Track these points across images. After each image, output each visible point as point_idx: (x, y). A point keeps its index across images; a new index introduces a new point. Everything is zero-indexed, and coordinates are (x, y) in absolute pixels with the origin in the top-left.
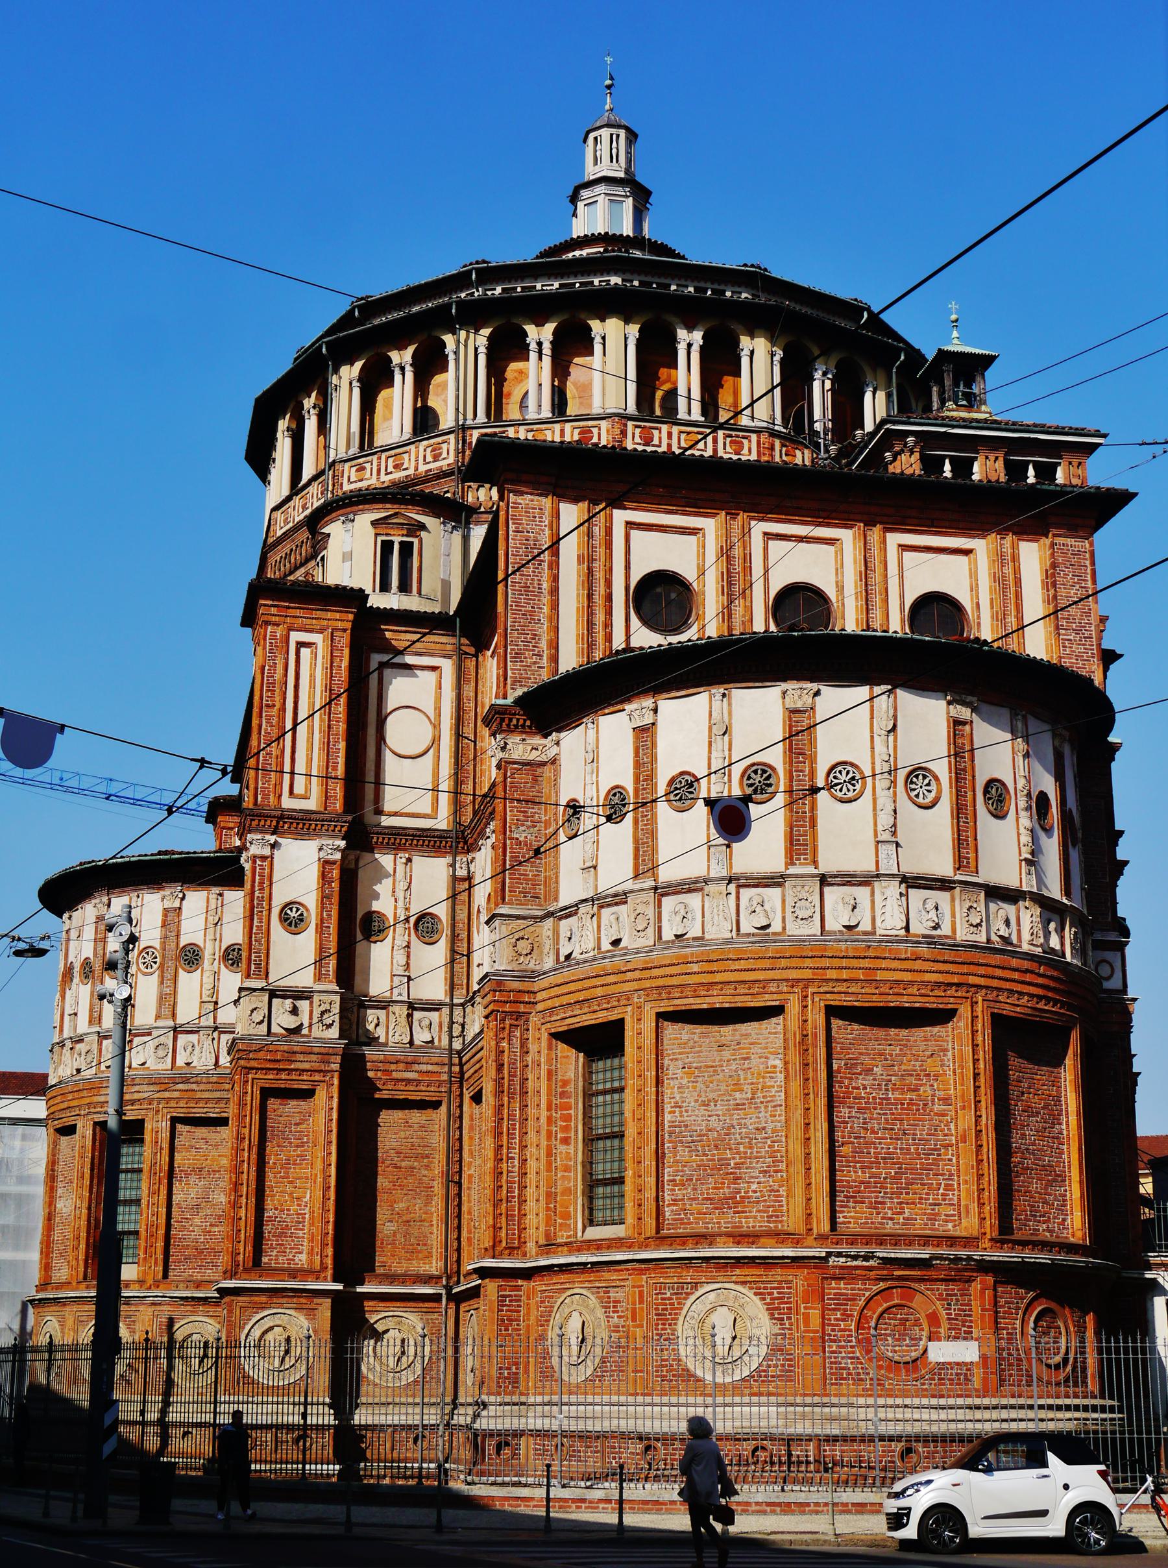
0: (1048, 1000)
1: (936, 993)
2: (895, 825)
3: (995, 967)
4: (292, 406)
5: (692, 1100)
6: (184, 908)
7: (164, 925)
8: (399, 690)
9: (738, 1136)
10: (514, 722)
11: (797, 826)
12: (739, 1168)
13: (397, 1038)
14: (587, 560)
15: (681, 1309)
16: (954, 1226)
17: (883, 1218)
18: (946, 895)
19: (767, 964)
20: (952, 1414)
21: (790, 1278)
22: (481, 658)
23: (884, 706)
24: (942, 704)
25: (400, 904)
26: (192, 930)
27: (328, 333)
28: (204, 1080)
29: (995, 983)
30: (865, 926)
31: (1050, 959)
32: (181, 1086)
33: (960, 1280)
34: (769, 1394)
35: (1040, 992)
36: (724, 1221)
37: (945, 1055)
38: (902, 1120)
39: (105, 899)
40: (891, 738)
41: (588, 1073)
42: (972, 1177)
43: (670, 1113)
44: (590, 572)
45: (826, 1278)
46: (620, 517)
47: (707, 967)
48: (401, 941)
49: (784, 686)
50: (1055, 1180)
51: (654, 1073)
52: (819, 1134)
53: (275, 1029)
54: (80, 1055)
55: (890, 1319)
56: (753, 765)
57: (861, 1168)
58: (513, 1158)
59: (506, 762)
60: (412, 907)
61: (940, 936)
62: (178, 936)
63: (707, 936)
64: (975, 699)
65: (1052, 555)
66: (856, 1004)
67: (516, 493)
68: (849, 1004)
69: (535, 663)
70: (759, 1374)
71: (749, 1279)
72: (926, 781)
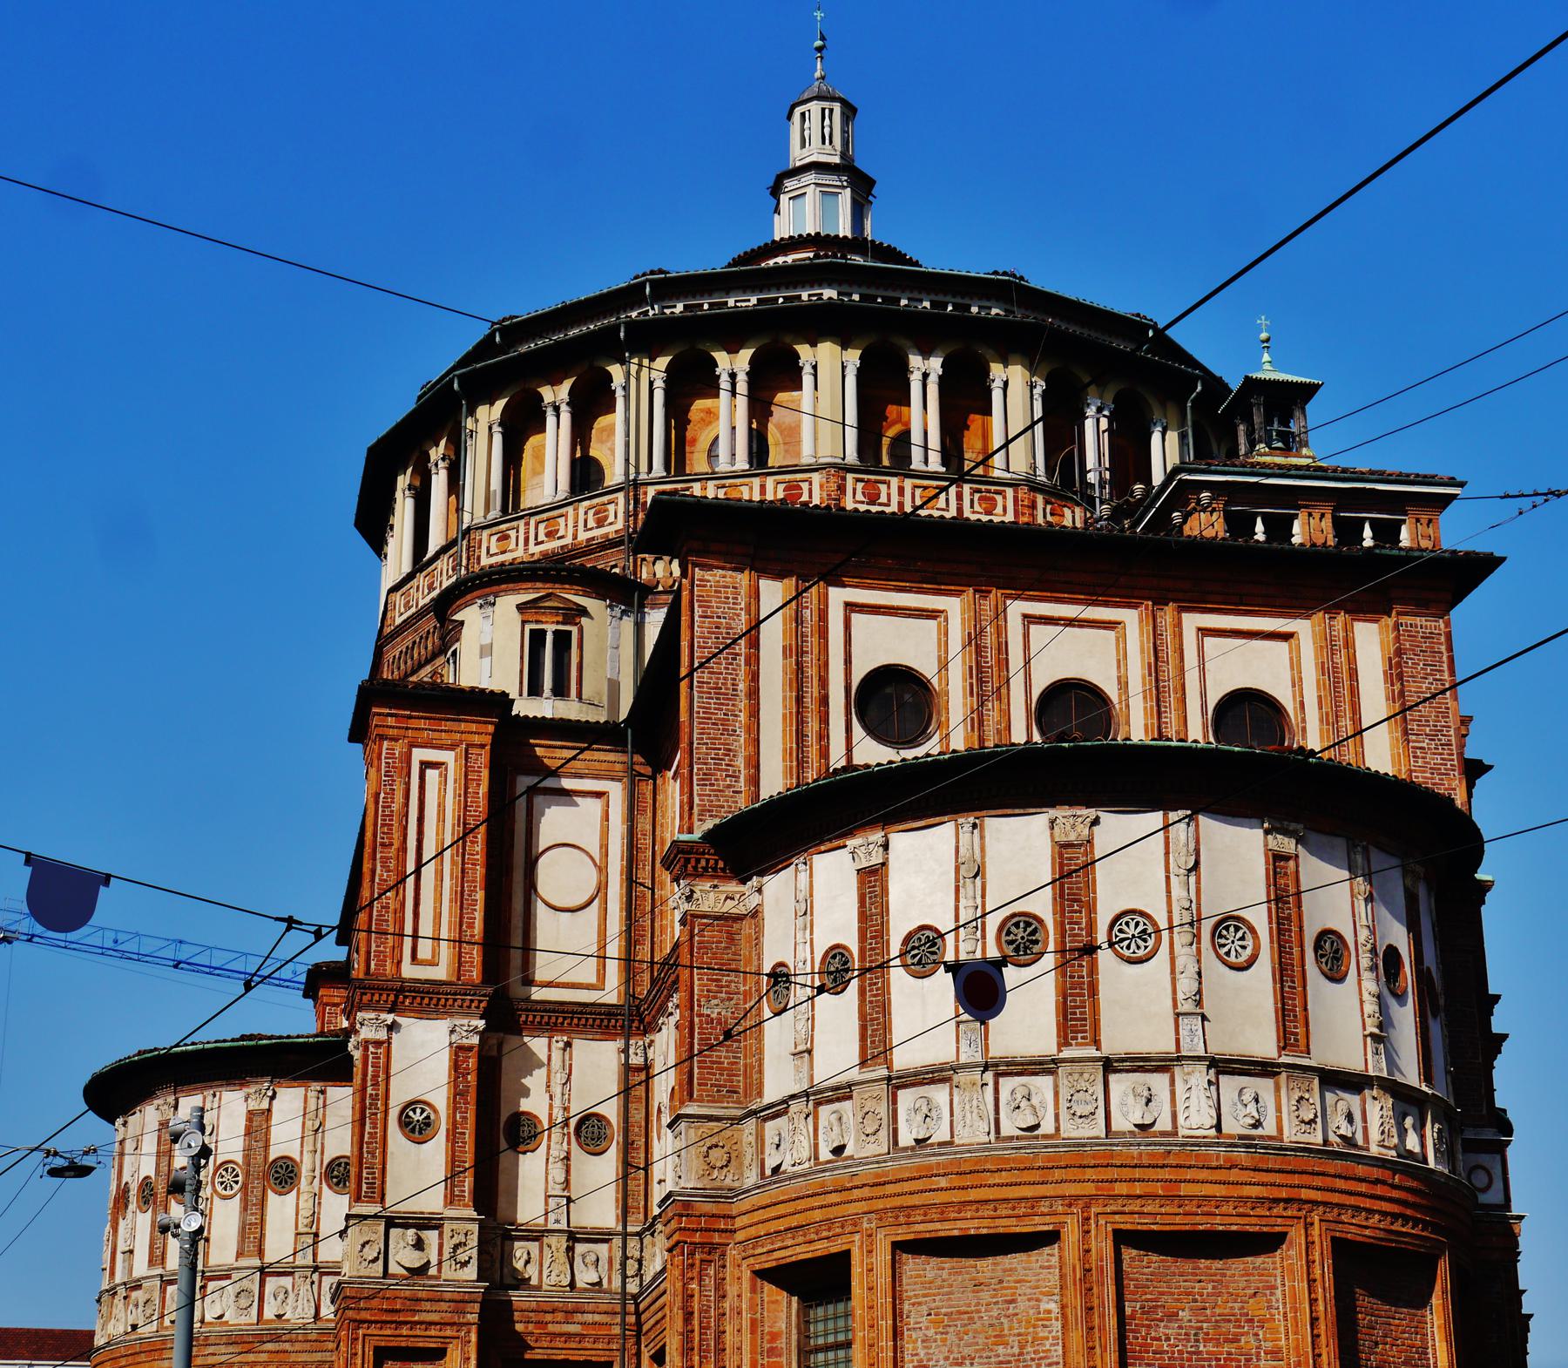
1: (1259, 1211)
2: (1199, 992)
3: (1334, 1176)
4: (414, 458)
5: (941, 1357)
6: (274, 1110)
7: (248, 1133)
8: (554, 823)
10: (703, 863)
11: (1071, 995)
13: (554, 1279)
14: (795, 652)
18: (1268, 1083)
19: (1035, 1176)
22: (659, 781)
23: (1183, 837)
24: (1258, 833)
25: (557, 1102)
26: (285, 1138)
27: (462, 363)
28: (300, 1338)
29: (1336, 1198)
30: (1164, 1124)
31: (1407, 1165)
32: (269, 1346)
35: (1396, 1209)
37: (1272, 1294)
39: (171, 1099)
40: (1192, 879)
41: (804, 1323)
44: (800, 667)
46: (838, 596)
48: (558, 1151)
49: (1053, 813)
51: (890, 1322)
53: (394, 1269)
54: (137, 1306)
56: (1014, 915)
59: (692, 915)
60: (572, 1105)
61: (1261, 1137)
62: (267, 1147)
63: (957, 1141)
64: (1300, 827)
65: (1397, 639)
66: (1154, 1227)
67: (704, 567)
68: (1145, 1228)
69: (729, 786)
72: (1240, 934)
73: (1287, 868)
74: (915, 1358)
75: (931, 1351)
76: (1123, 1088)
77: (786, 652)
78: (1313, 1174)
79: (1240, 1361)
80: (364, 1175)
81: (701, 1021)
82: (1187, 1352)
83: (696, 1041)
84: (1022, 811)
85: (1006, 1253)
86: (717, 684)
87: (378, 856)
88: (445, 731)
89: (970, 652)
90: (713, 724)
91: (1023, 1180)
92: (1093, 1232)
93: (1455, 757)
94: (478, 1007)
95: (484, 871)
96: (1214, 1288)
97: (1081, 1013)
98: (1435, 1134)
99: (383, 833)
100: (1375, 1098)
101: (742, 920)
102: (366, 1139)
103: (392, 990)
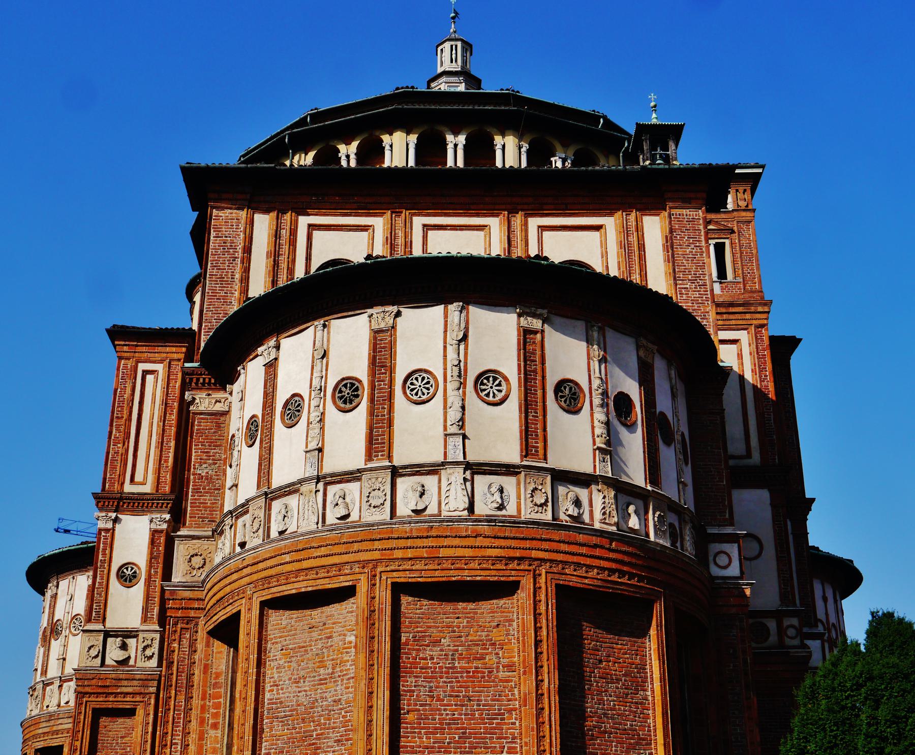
0: (622, 574)
1: (498, 566)
2: (462, 420)
3: (559, 542)
5: (287, 678)
9: (320, 709)
10: (201, 380)
11: (377, 428)
12: (319, 739)
18: (512, 480)
19: (341, 548)
23: (456, 320)
29: (560, 557)
30: (432, 510)
31: (624, 537)
35: (613, 566)
37: (510, 625)
38: (467, 687)
39: (55, 583)
40: (462, 347)
43: (269, 691)
46: (304, 221)
47: (295, 556)
49: (370, 311)
50: (637, 743)
52: (380, 702)
53: (108, 661)
57: (426, 733)
58: (176, 744)
61: (504, 516)
64: (545, 311)
66: (419, 579)
67: (218, 208)
68: (413, 580)
72: (497, 382)
73: (535, 339)
74: (272, 680)
75: (281, 675)
76: (405, 486)
77: (268, 255)
78: (541, 540)
79: (484, 673)
80: (94, 607)
81: (195, 478)
82: (446, 668)
83: (190, 490)
84: (352, 313)
85: (328, 605)
86: (222, 275)
87: (114, 424)
88: (157, 353)
89: (387, 248)
90: (218, 299)
92: (378, 585)
93: (709, 293)
94: (166, 507)
95: (175, 429)
96: (468, 622)
97: (382, 439)
98: (656, 519)
99: (118, 411)
100: (599, 491)
101: (226, 414)
102: (97, 586)
103: (115, 499)
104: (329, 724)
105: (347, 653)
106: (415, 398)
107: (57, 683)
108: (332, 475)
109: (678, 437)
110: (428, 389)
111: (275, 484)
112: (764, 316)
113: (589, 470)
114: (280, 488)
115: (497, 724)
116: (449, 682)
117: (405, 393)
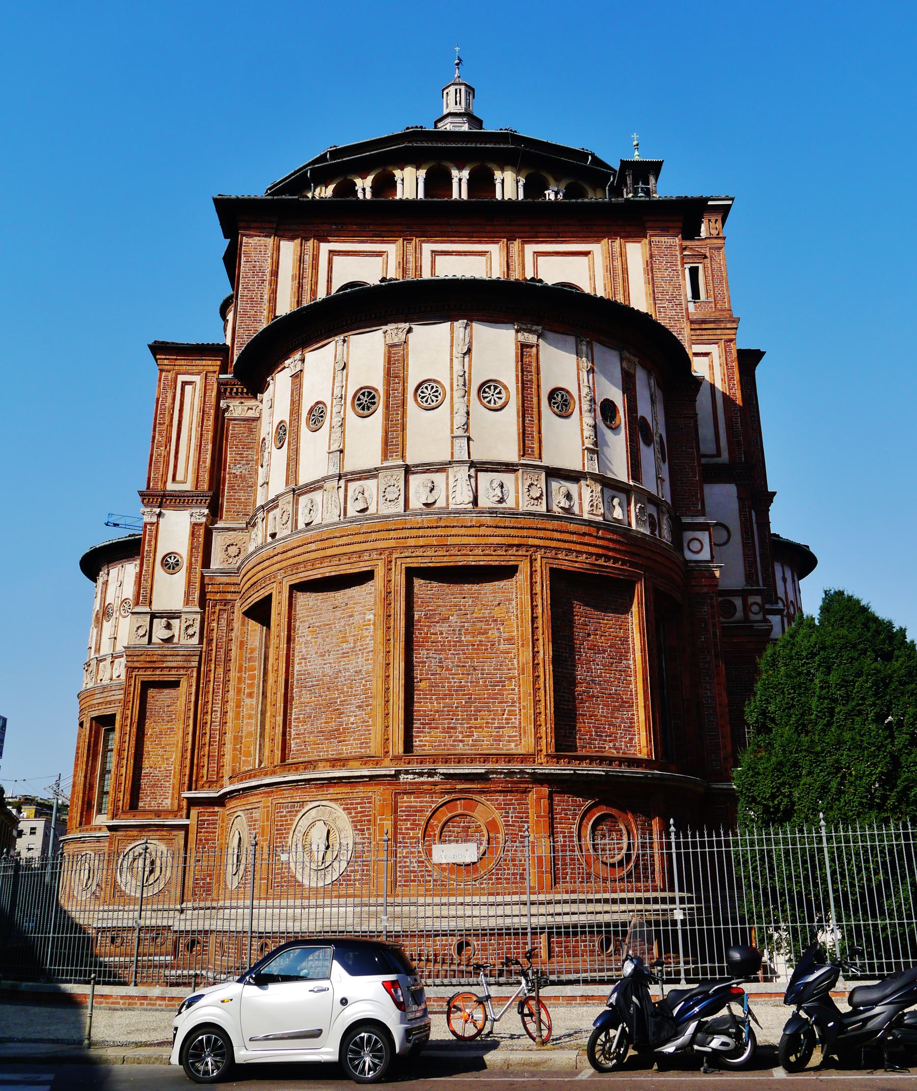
0: (608, 558)
2: (467, 424)
3: (553, 530)
5: (313, 652)
12: (343, 705)
15: (292, 824)
16: (516, 746)
17: (454, 741)
18: (511, 476)
20: (508, 910)
21: (370, 794)
29: (554, 544)
31: (609, 526)
33: (517, 791)
34: (347, 896)
35: (600, 551)
36: (331, 750)
40: (467, 359)
42: (528, 702)
43: (298, 664)
45: (400, 793)
50: (621, 706)
52: (396, 672)
53: (154, 640)
55: (454, 827)
58: (216, 711)
61: (505, 508)
70: (344, 878)
71: (339, 796)
72: (497, 391)
78: (537, 529)
80: (142, 592)
85: (350, 587)
91: (354, 541)
92: (393, 569)
98: (637, 510)
100: (588, 486)
104: (352, 692)
105: (367, 629)
106: (425, 404)
107: (109, 659)
108: (352, 473)
109: (656, 438)
110: (437, 397)
111: (302, 481)
112: (733, 331)
113: (579, 468)
114: (306, 485)
115: (499, 690)
116: (457, 654)
117: (416, 400)
